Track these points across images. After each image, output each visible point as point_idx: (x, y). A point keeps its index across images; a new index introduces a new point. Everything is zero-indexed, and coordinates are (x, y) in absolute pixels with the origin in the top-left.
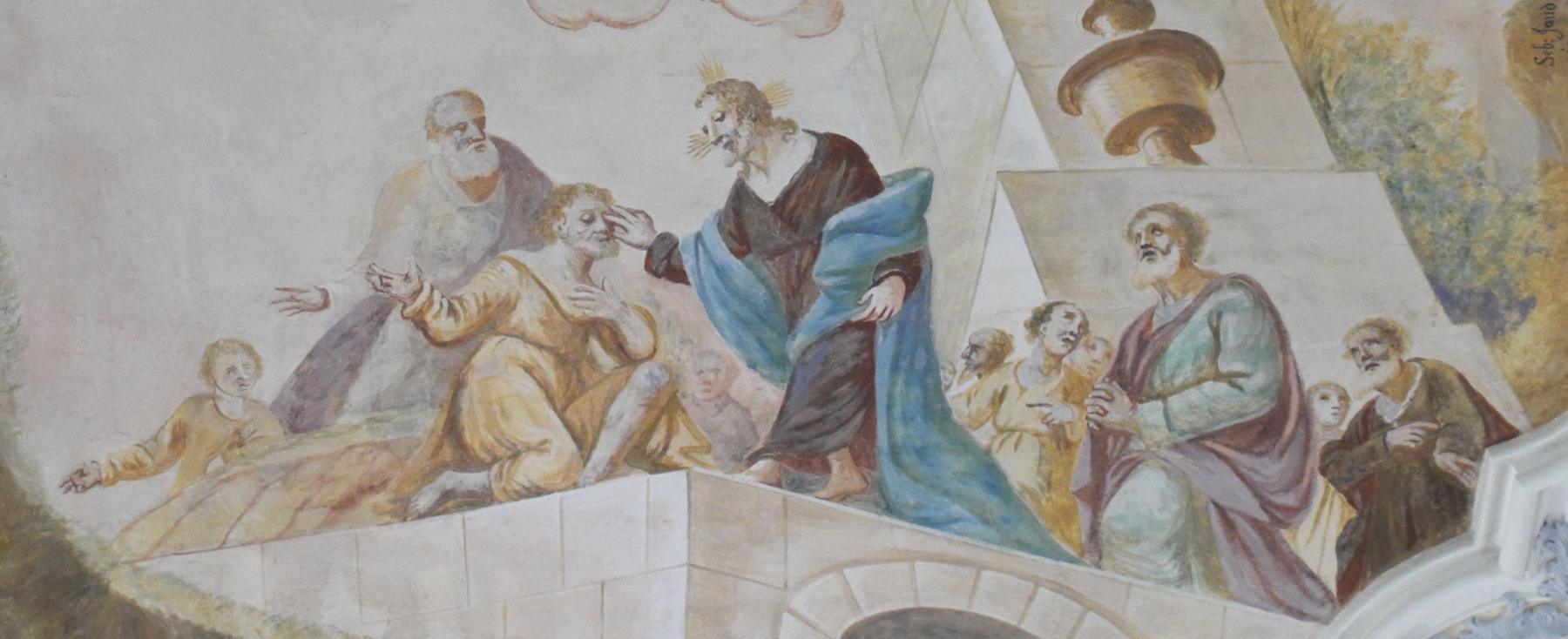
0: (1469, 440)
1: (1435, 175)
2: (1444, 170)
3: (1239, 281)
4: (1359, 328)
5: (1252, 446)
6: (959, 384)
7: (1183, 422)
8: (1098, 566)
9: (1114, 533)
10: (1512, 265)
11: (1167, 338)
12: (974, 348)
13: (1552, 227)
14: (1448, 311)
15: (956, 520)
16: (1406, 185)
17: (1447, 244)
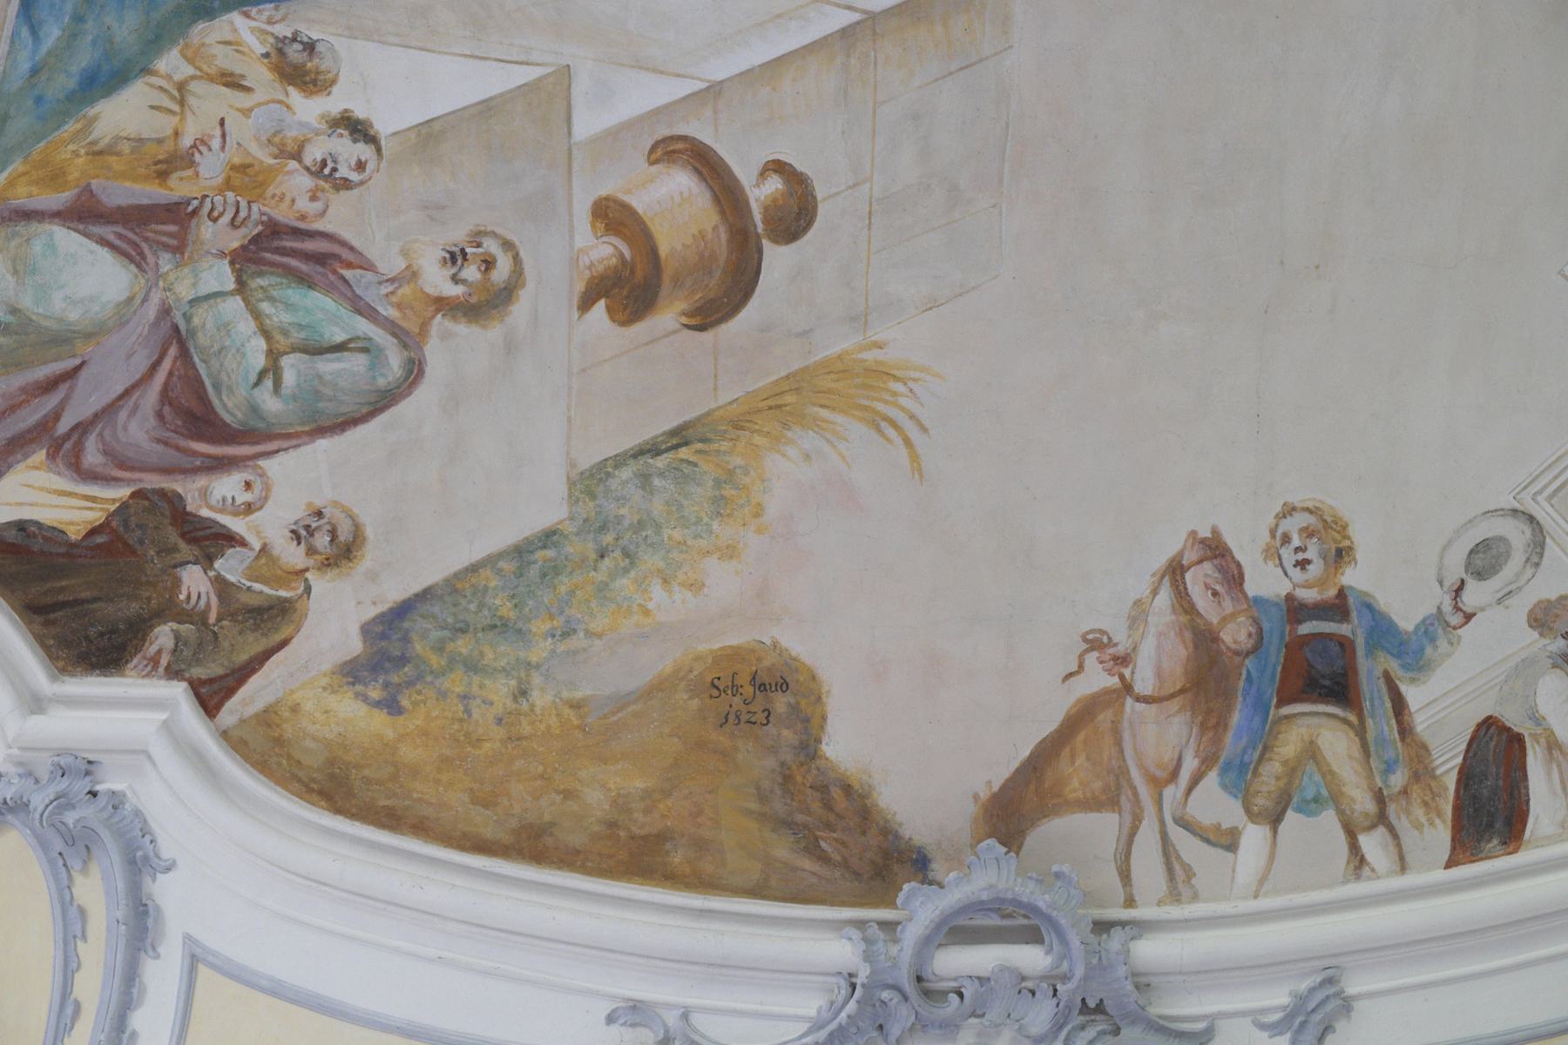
0: (197, 661)
1: (564, 584)
2: (572, 593)
3: (415, 372)
4: (352, 517)
5: (170, 404)
6: (253, 30)
7: (203, 318)
9: (28, 240)
10: (445, 683)
11: (329, 289)
12: (310, 47)
13: (499, 721)
14: (381, 619)
15: (34, 32)
16: (550, 553)
17: (473, 607)
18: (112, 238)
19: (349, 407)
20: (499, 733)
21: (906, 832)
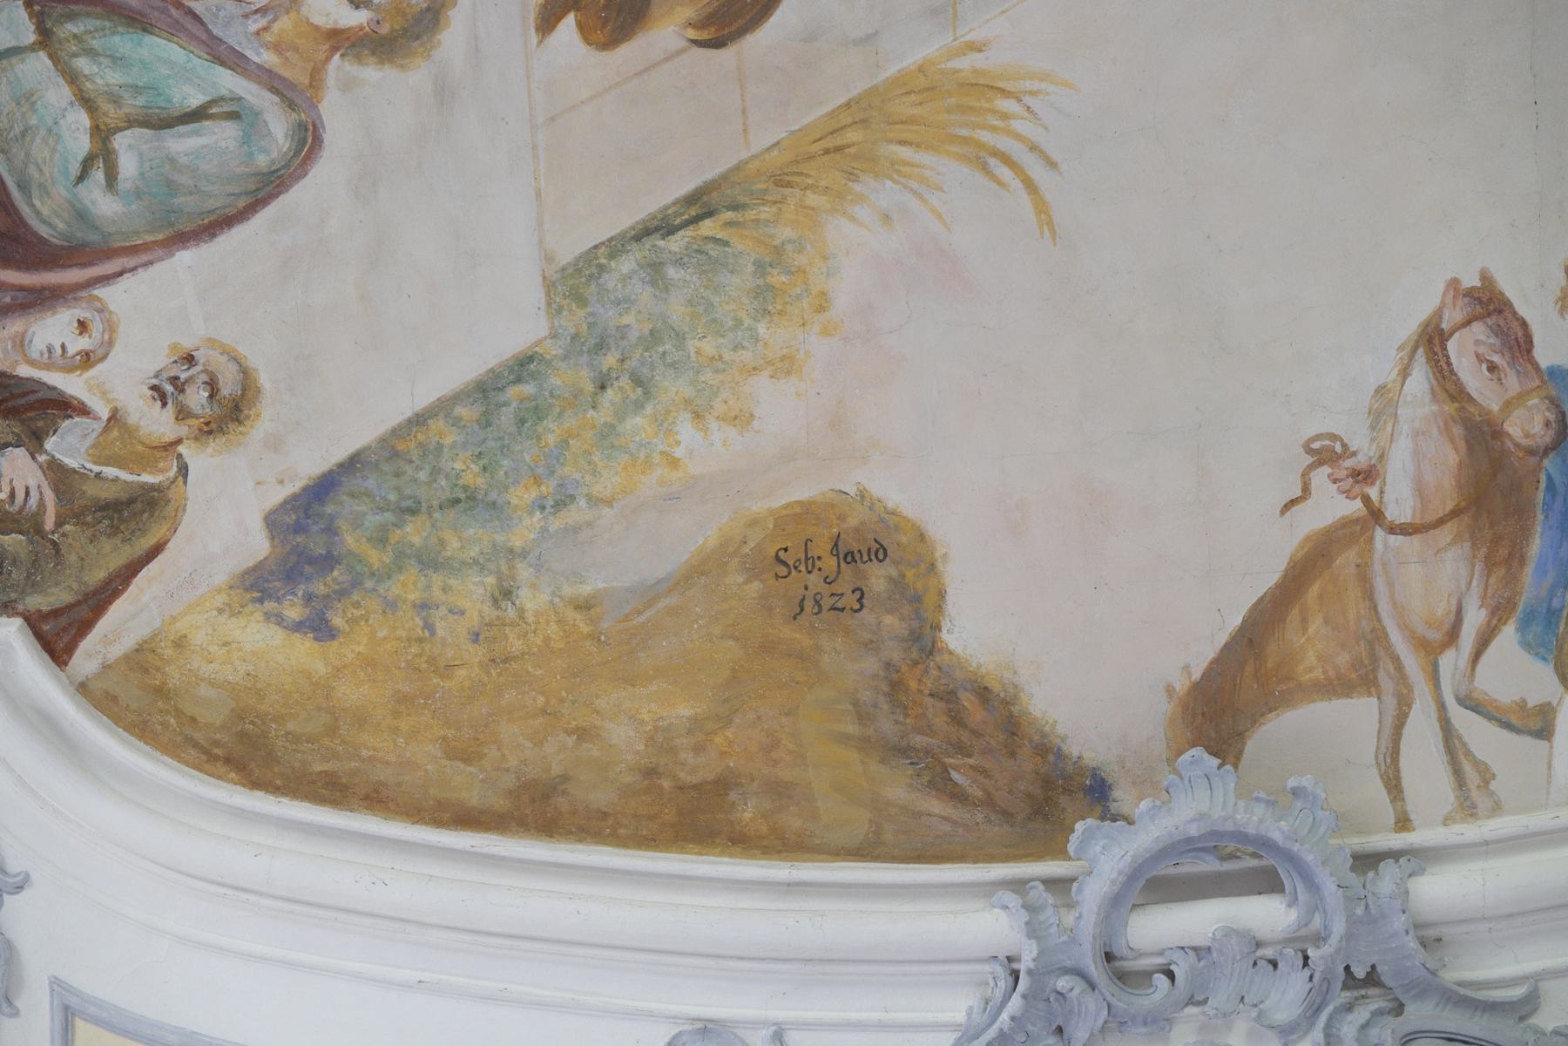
0: (32, 585)
1: (552, 431)
2: (564, 444)
3: (308, 142)
4: (235, 359)
10: (394, 589)
14: (291, 503)
16: (528, 389)
17: (423, 476)
19: (217, 199)
20: (477, 654)
21: (1073, 749)
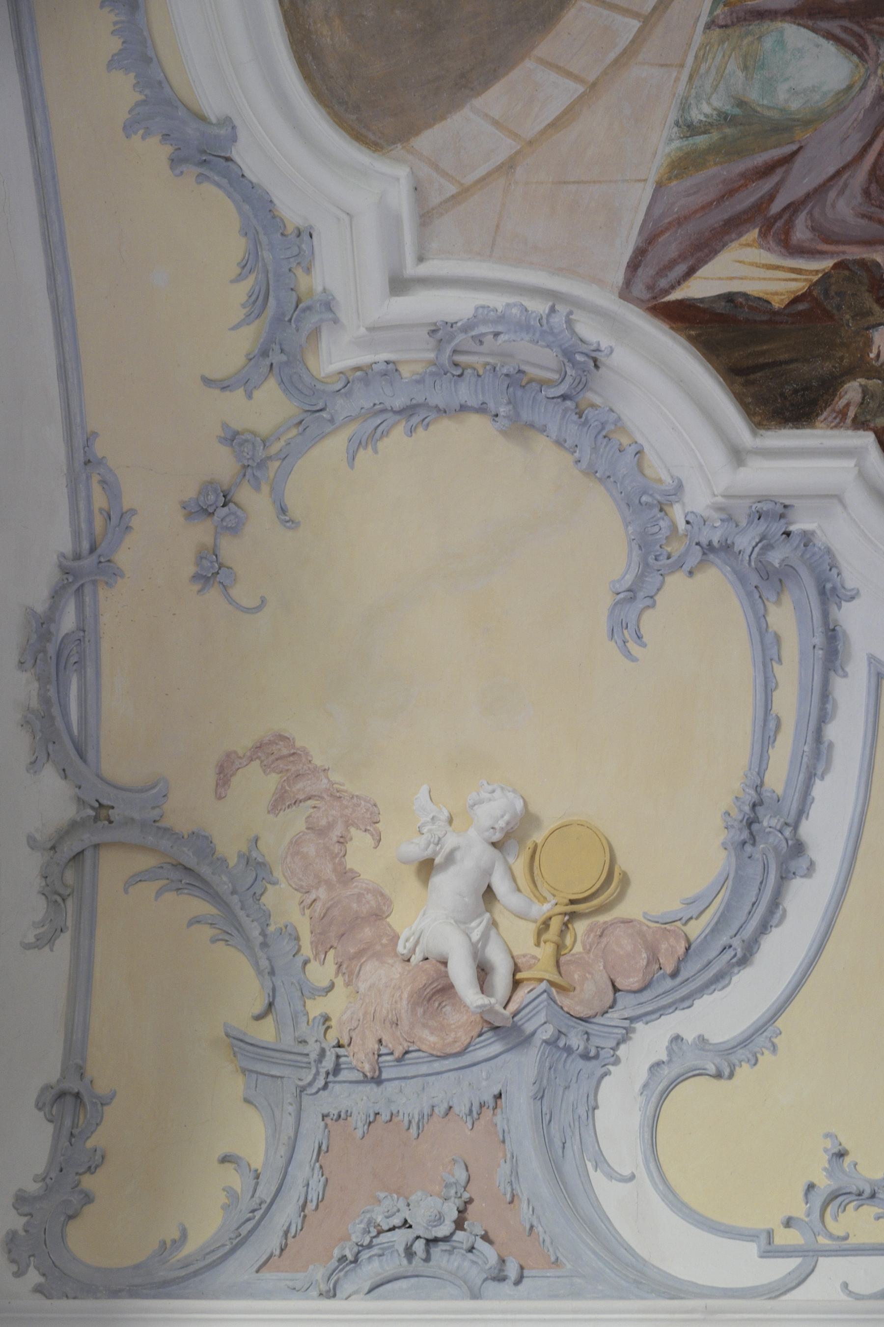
5: (877, 182)
8: (709, 26)
9: (759, 38)
18: (838, 31)
